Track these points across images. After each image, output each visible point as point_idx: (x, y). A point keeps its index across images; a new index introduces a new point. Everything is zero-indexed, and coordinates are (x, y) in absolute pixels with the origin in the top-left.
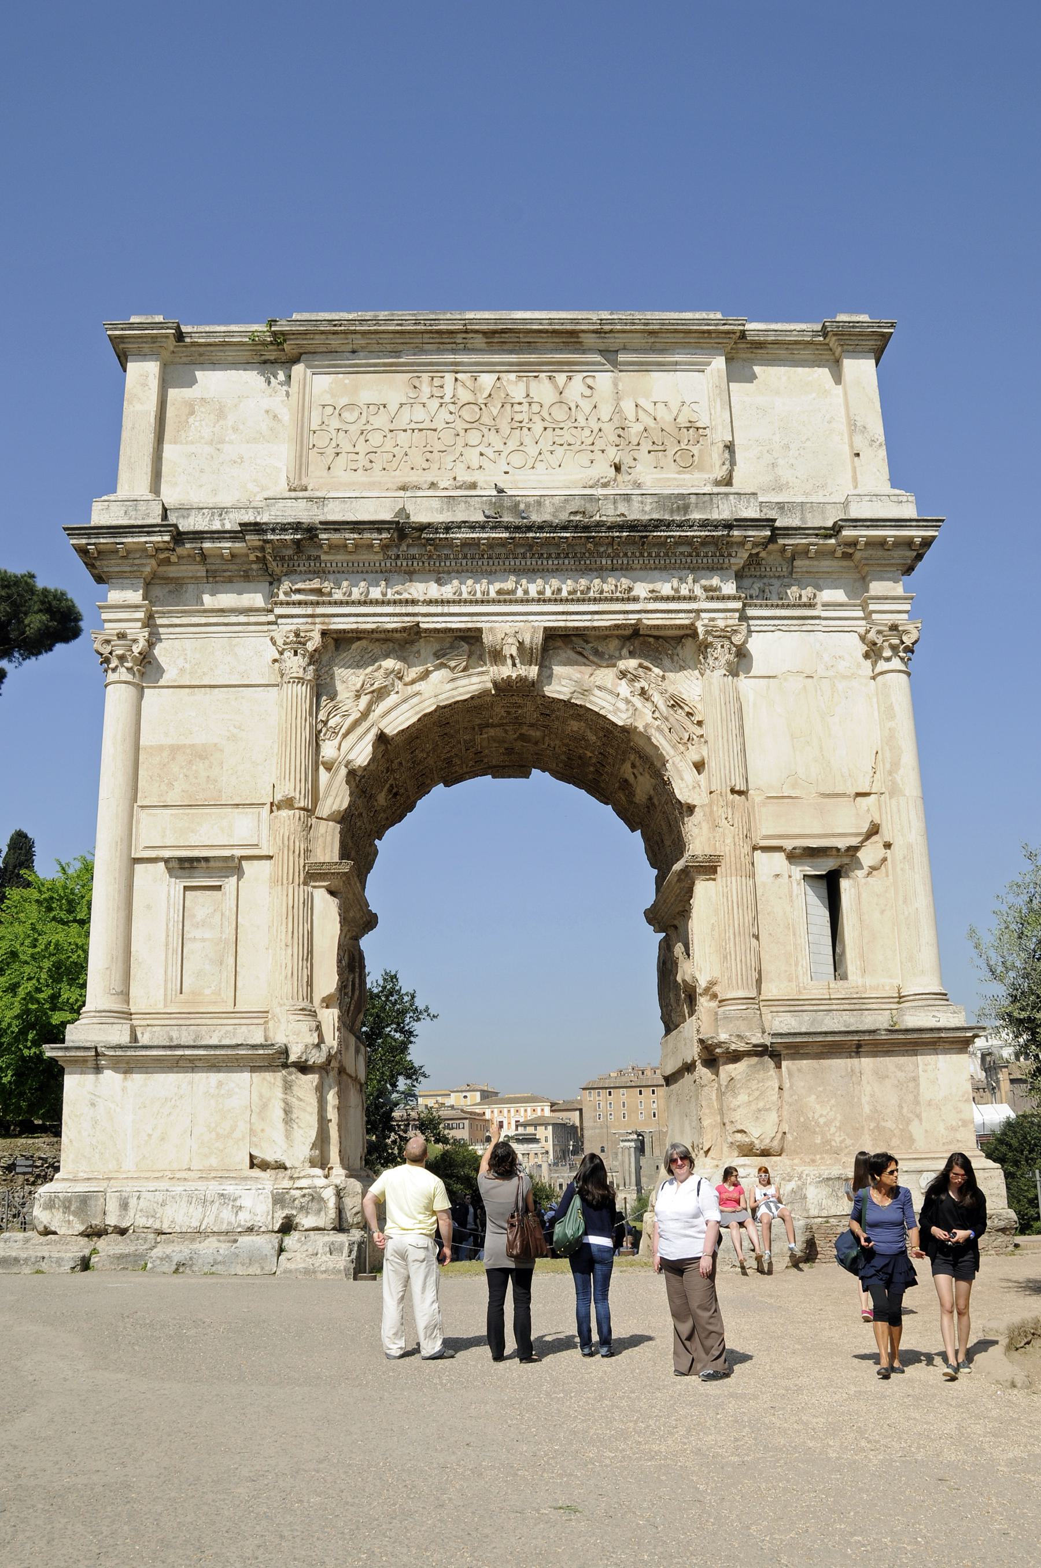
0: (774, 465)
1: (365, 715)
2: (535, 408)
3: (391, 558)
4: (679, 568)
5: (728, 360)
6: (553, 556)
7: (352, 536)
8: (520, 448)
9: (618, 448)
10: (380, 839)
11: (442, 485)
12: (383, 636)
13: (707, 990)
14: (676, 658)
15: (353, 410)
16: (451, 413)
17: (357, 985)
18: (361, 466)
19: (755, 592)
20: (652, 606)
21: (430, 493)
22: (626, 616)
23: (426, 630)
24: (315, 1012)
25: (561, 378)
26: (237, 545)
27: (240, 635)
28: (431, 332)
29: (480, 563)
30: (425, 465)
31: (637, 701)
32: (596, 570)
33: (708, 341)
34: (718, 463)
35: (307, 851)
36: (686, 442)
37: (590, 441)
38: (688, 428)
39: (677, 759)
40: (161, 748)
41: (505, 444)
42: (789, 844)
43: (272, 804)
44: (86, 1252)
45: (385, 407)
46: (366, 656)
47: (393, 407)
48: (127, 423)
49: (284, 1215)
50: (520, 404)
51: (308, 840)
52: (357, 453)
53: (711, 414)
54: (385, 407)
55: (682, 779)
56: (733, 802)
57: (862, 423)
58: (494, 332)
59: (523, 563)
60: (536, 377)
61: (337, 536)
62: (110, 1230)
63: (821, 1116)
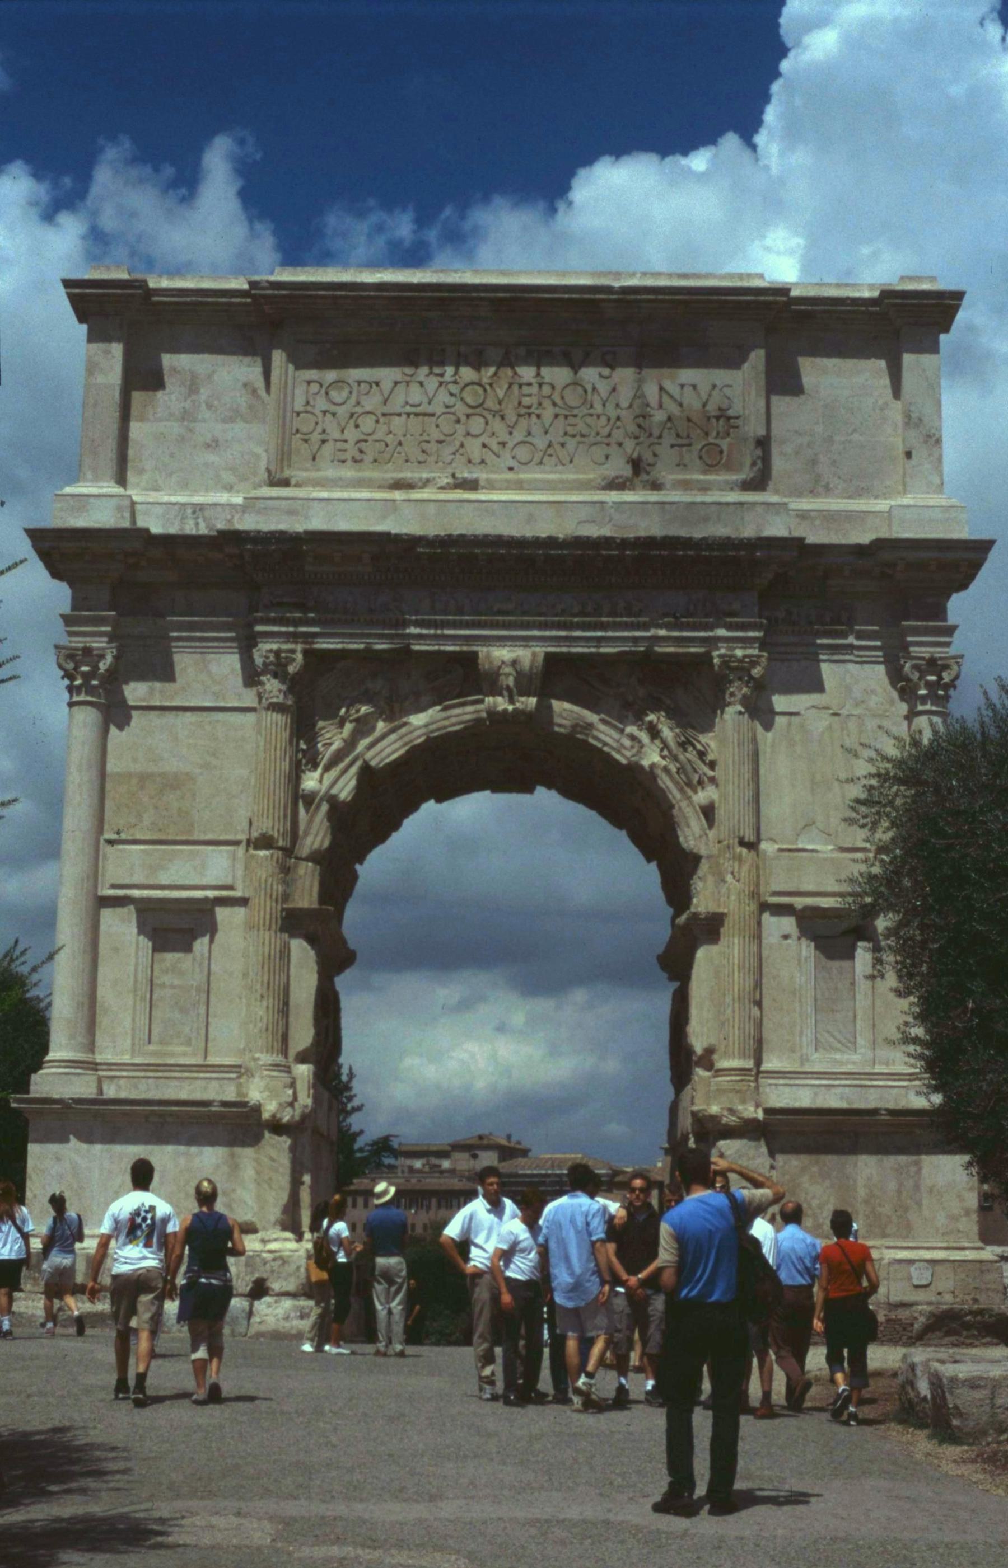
0: (814, 462)
1: (350, 744)
2: (546, 390)
8: (529, 439)
13: (701, 1058)
15: (342, 388)
16: (452, 394)
18: (348, 456)
24: (289, 1067)
30: (422, 457)
31: (644, 737)
34: (748, 462)
35: (286, 897)
36: (714, 434)
37: (607, 430)
38: (718, 418)
39: (684, 804)
40: (129, 775)
42: (799, 902)
43: (248, 842)
47: (387, 385)
49: (253, 1279)
50: (530, 384)
51: (285, 882)
52: (346, 441)
53: (744, 401)
54: (377, 384)
55: (688, 826)
56: (740, 855)
57: (917, 414)
63: (814, 1197)
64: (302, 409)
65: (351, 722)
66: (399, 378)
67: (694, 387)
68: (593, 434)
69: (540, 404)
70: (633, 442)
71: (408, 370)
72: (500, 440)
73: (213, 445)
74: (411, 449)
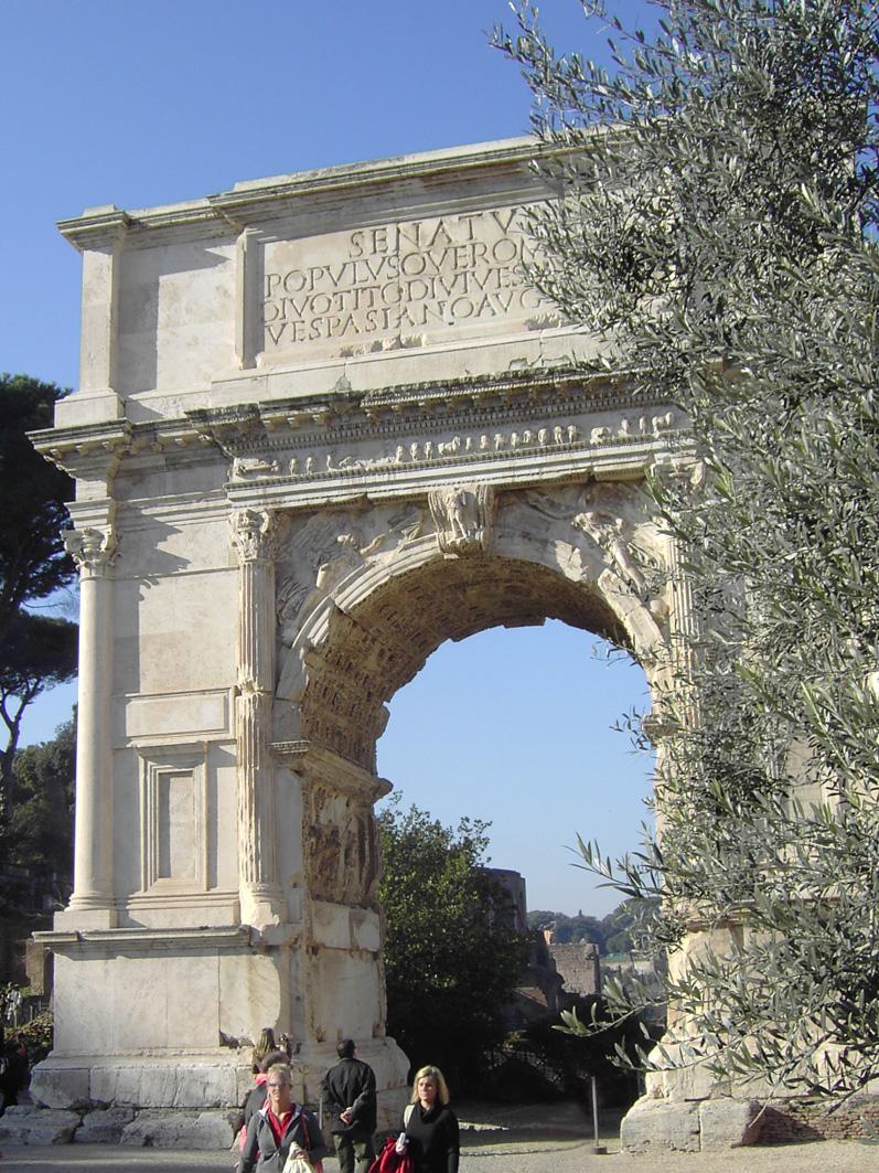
2: (479, 250)
4: (631, 407)
7: (292, 413)
8: (464, 295)
10: (389, 701)
11: (386, 345)
12: (336, 508)
14: (637, 502)
17: (367, 853)
20: (600, 452)
21: (375, 356)
22: (576, 465)
23: (377, 499)
25: (505, 213)
26: (188, 432)
27: (202, 520)
28: (367, 184)
29: (423, 425)
32: (543, 418)
41: (449, 293)
44: (71, 1126)
46: (323, 530)
48: (86, 319)
50: (464, 247)
52: (303, 322)
58: (431, 175)
59: (467, 420)
60: (480, 215)
61: (278, 414)
62: (95, 1104)
65: (323, 570)
66: (347, 260)
69: (474, 263)
73: (194, 343)
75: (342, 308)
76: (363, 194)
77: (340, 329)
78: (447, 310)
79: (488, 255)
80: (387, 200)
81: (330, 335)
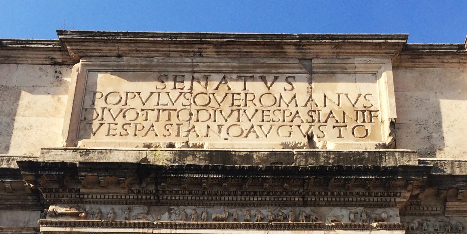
0: (429, 138)
2: (250, 97)
3: (134, 193)
5: (395, 68)
6: (258, 193)
8: (238, 123)
9: (310, 124)
19: (415, 225)
32: (291, 206)
33: (379, 51)
36: (362, 120)
37: (291, 118)
41: (226, 120)
45: (139, 94)
50: (239, 94)
52: (116, 124)
58: (222, 44)
60: (251, 77)
64: (89, 107)
66: (154, 90)
67: (347, 95)
68: (281, 120)
70: (308, 125)
71: (160, 85)
72: (219, 124)
74: (159, 128)
75: (147, 120)
76: (171, 49)
77: (144, 132)
78: (224, 130)
79: (256, 101)
80: (188, 57)
81: (136, 135)
